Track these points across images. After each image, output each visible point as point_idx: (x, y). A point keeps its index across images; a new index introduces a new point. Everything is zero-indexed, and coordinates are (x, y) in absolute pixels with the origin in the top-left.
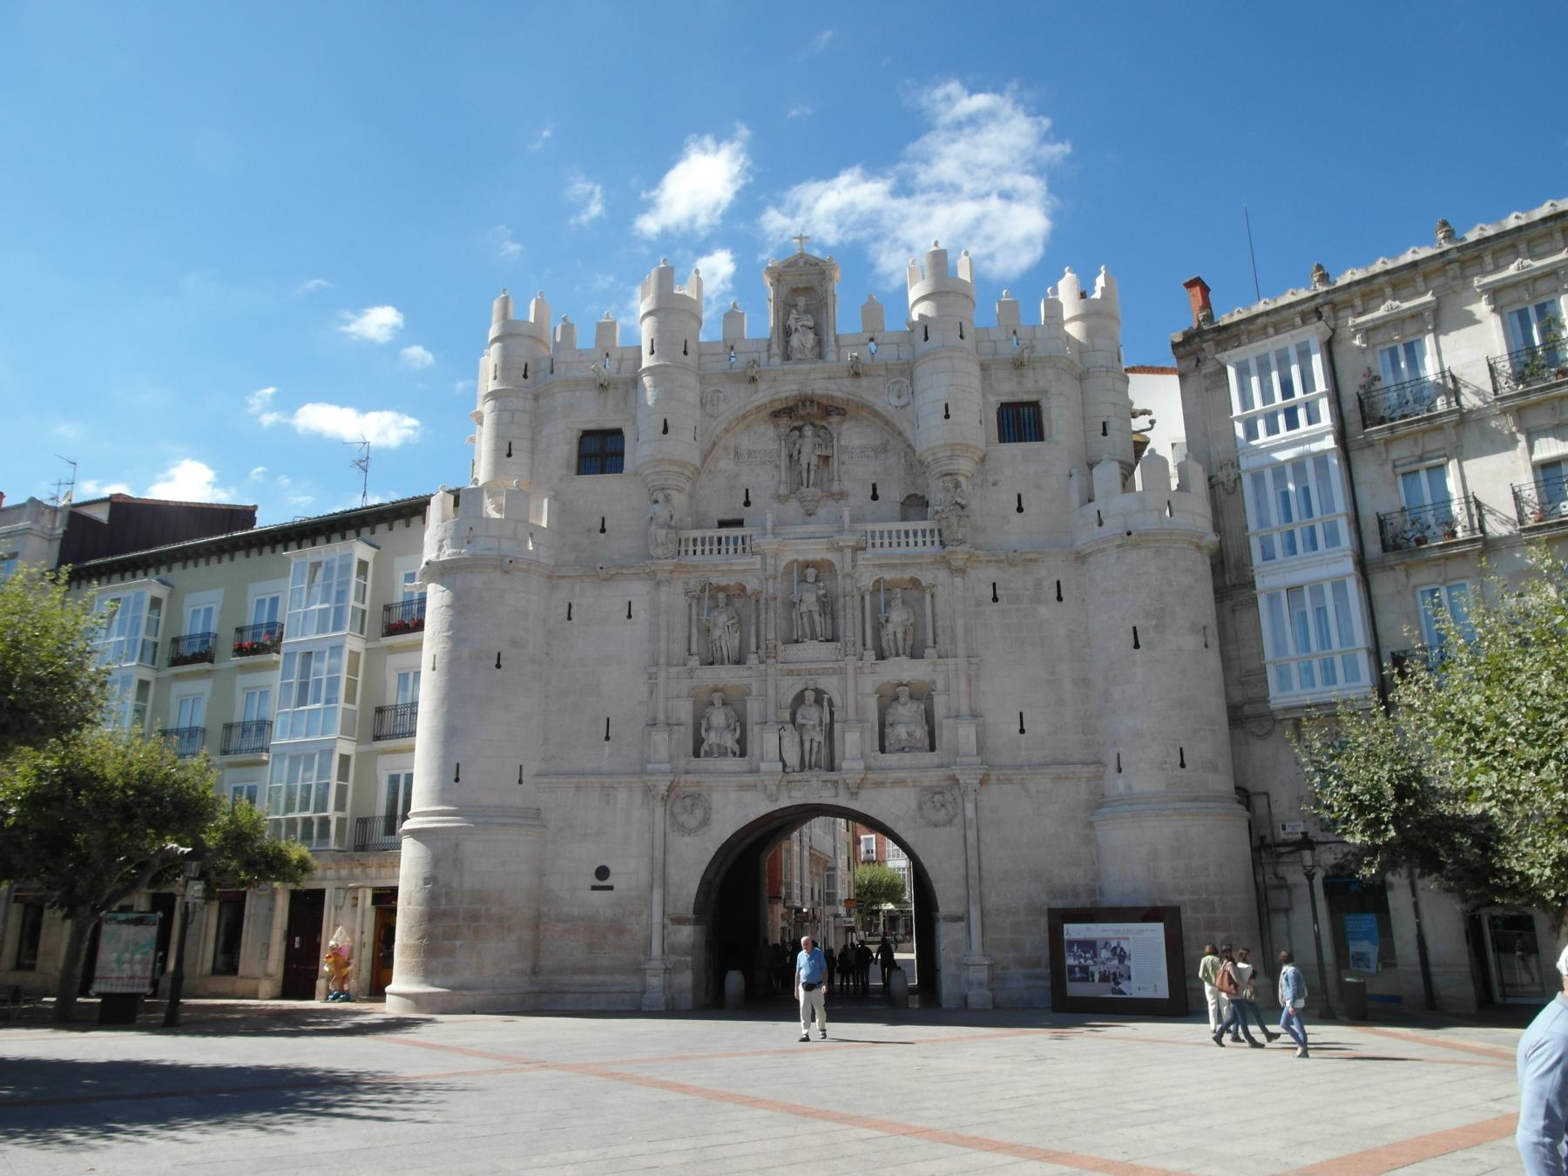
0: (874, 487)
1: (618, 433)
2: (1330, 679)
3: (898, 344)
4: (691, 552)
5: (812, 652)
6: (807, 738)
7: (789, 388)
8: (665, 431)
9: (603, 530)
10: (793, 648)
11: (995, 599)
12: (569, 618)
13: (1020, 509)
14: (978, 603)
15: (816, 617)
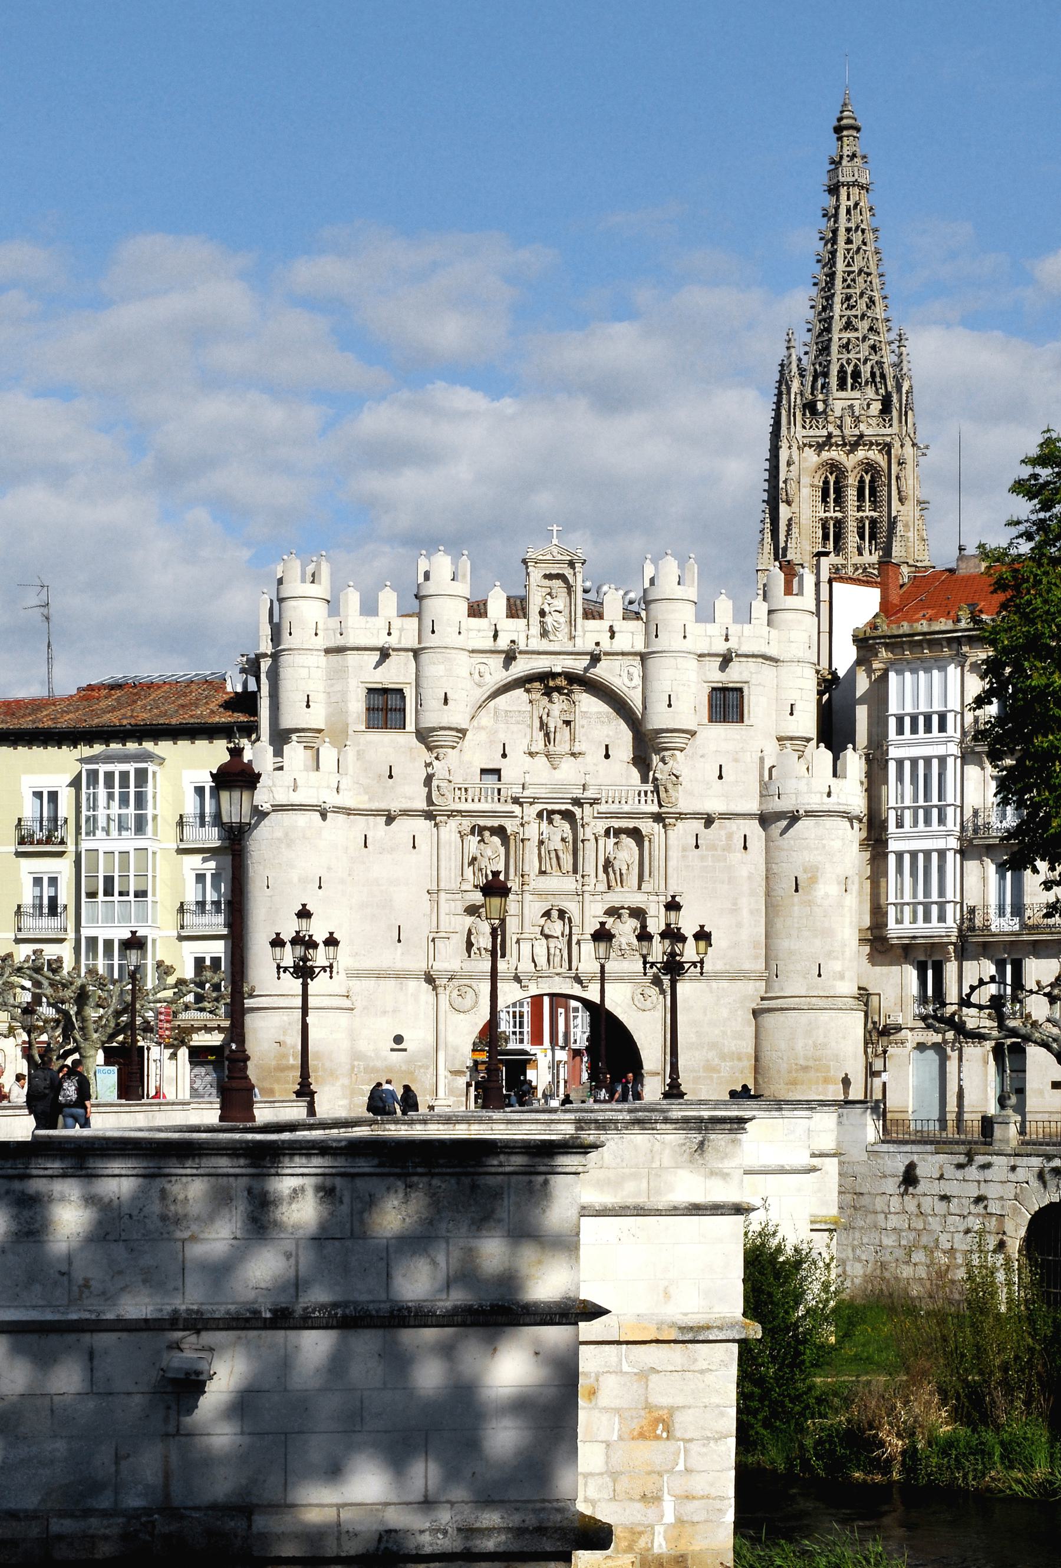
0: (607, 746)
1: (400, 691)
2: (927, 919)
3: (633, 633)
4: (463, 800)
5: (556, 882)
6: (552, 945)
7: (541, 664)
8: (446, 702)
9: (391, 777)
10: (542, 878)
11: (697, 847)
12: (366, 846)
13: (720, 777)
14: (684, 850)
15: (560, 854)
